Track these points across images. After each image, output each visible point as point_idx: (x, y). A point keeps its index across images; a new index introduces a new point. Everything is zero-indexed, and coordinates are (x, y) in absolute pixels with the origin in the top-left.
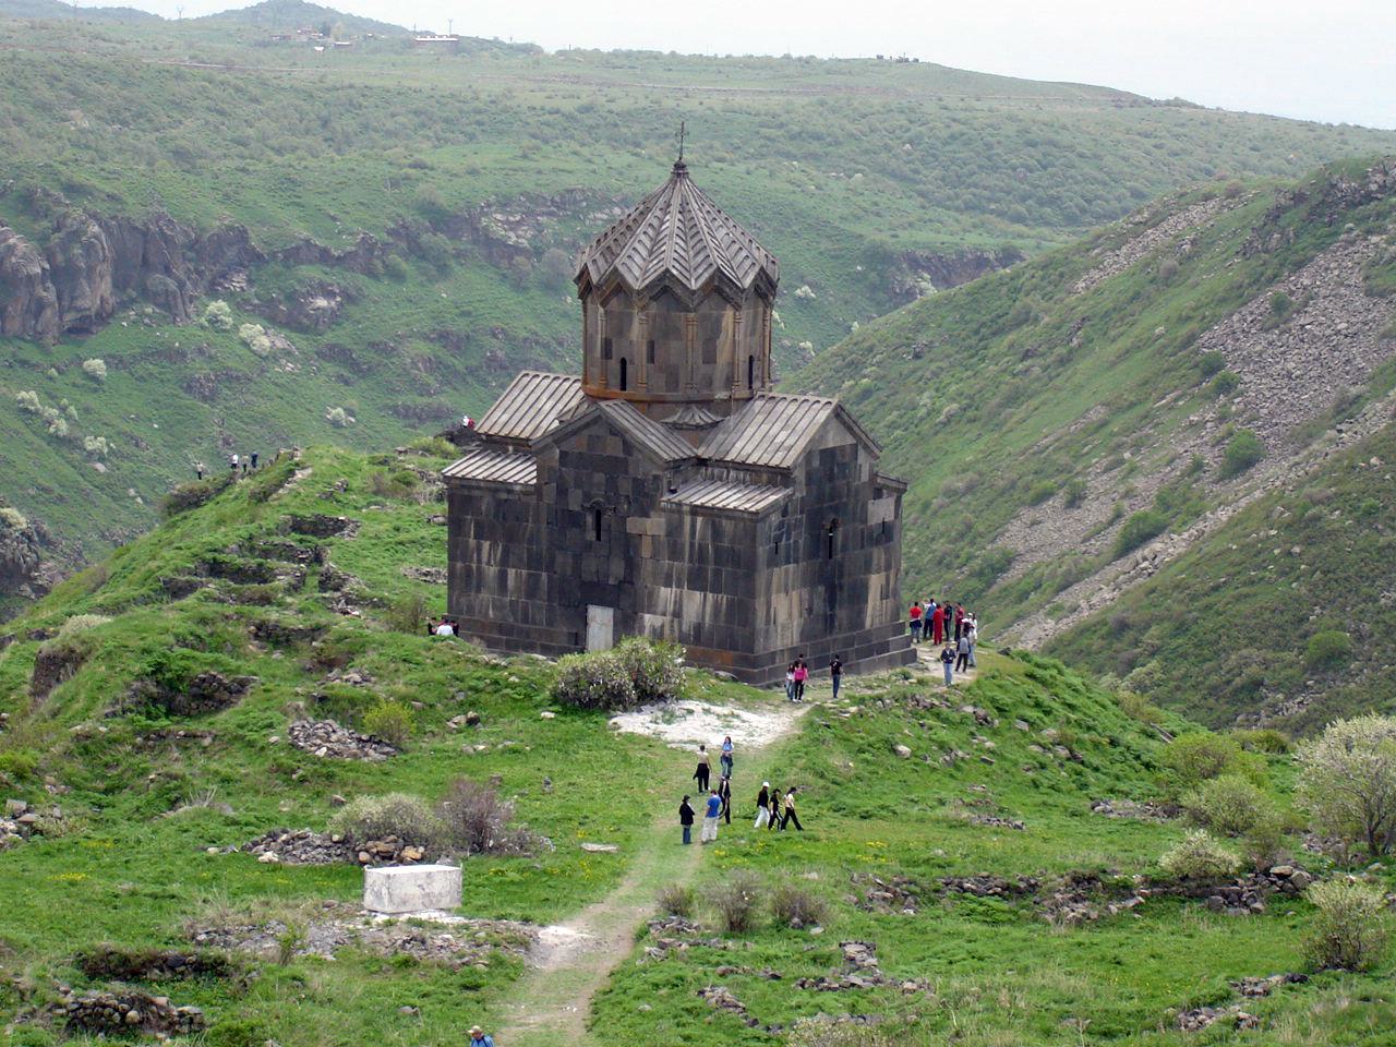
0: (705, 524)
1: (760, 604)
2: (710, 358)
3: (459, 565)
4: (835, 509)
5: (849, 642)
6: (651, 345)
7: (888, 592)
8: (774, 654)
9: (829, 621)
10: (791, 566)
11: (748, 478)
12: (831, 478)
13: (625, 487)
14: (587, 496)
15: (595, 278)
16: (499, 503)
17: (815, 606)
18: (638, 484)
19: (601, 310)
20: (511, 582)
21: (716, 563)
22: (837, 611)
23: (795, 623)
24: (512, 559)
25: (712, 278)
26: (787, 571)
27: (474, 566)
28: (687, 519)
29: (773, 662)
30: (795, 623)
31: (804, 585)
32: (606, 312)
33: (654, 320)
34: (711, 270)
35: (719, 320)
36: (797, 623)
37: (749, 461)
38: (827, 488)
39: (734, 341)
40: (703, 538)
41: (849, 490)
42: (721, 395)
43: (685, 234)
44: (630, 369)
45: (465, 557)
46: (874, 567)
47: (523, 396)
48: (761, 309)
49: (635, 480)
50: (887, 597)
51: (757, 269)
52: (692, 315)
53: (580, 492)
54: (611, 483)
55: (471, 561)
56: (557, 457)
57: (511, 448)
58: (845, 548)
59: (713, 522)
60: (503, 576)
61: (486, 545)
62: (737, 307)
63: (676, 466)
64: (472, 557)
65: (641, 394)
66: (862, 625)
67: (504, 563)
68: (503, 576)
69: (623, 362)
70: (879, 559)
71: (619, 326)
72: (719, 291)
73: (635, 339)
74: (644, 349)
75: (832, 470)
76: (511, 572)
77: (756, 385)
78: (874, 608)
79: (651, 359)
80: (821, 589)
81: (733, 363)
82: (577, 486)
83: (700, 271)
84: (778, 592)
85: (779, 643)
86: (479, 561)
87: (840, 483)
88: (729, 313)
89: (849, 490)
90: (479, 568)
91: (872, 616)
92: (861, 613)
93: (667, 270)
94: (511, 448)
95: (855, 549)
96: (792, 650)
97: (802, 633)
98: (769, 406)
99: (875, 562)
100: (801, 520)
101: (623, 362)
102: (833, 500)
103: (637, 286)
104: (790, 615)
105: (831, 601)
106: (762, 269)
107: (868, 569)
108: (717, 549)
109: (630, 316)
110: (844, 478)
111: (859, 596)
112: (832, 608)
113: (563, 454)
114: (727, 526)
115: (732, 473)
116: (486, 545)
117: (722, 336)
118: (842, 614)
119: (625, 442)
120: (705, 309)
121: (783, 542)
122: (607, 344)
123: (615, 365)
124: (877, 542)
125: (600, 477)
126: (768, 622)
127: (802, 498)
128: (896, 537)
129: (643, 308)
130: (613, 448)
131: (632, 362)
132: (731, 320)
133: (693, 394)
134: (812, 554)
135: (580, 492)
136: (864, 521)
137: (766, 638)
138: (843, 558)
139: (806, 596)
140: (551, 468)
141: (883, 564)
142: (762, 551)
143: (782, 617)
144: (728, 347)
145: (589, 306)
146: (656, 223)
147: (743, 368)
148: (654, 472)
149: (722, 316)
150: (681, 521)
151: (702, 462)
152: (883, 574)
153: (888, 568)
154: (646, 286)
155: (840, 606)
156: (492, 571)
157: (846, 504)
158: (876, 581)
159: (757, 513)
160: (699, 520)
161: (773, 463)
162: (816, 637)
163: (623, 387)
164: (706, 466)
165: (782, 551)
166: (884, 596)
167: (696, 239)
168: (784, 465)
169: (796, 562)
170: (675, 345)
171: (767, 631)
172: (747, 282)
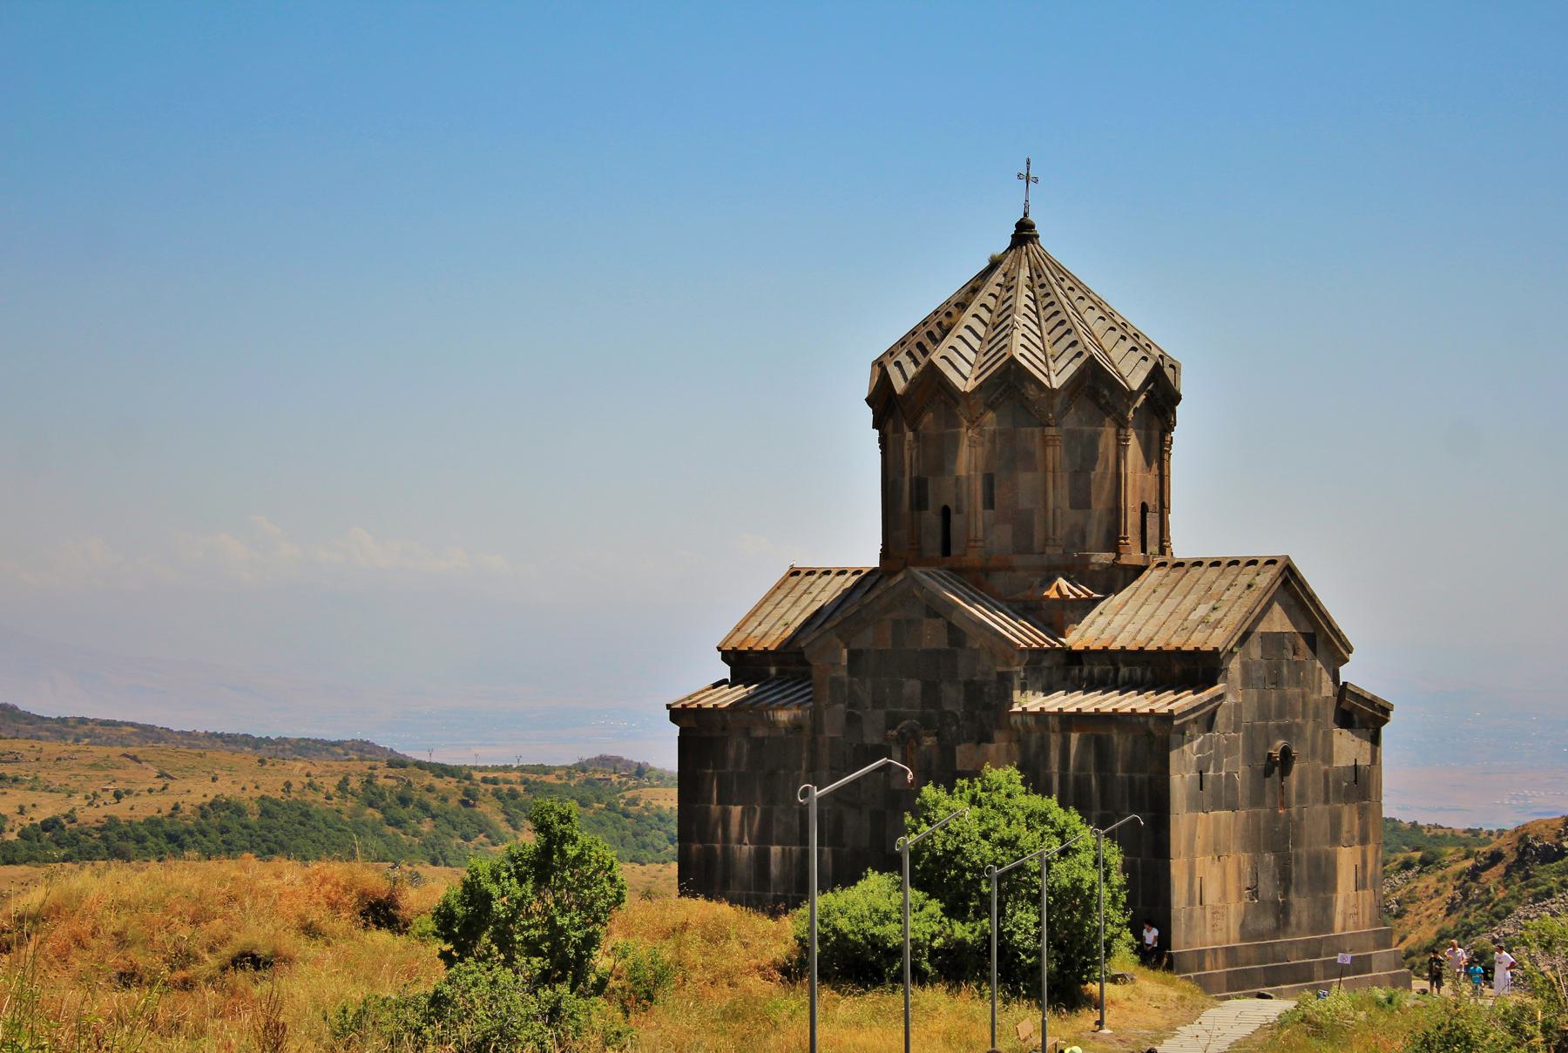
0: (1083, 743)
1: (1178, 868)
2: (1081, 501)
3: (695, 847)
4: (1285, 732)
5: (1312, 949)
6: (989, 481)
7: (1364, 878)
8: (1201, 953)
9: (1282, 912)
10: (1224, 814)
11: (1149, 674)
12: (1277, 682)
13: (953, 699)
14: (893, 721)
15: (899, 385)
16: (757, 744)
17: (1261, 885)
18: (973, 691)
19: (909, 435)
20: (774, 870)
21: (1103, 807)
22: (1293, 897)
23: (1232, 908)
24: (776, 830)
25: (1081, 372)
26: (1216, 819)
27: (718, 846)
28: (1055, 740)
29: (1201, 967)
30: (1232, 908)
31: (1245, 851)
32: (917, 438)
33: (993, 442)
34: (1079, 362)
35: (1093, 441)
36: (1234, 910)
37: (1152, 647)
38: (1274, 696)
39: (1118, 475)
40: (1081, 767)
41: (1305, 705)
42: (1103, 558)
43: (1037, 314)
44: (955, 518)
45: (705, 835)
46: (1344, 835)
47: (791, 599)
48: (1156, 434)
49: (969, 684)
50: (1364, 887)
51: (1150, 364)
52: (1051, 431)
53: (881, 713)
54: (931, 691)
55: (713, 839)
56: (845, 662)
57: (773, 670)
58: (1301, 797)
59: (1098, 740)
60: (762, 858)
61: (736, 811)
62: (1121, 424)
63: (1035, 656)
64: (715, 832)
65: (973, 558)
66: (1331, 929)
67: (763, 839)
68: (762, 858)
69: (946, 512)
70: (1352, 825)
71: (940, 455)
72: (1094, 395)
73: (964, 473)
74: (978, 487)
75: (1279, 668)
76: (775, 850)
77: (1153, 548)
78: (1346, 901)
79: (989, 502)
80: (1269, 858)
81: (1118, 508)
82: (878, 704)
83: (1061, 363)
84: (1205, 853)
85: (1208, 933)
86: (726, 838)
87: (1292, 691)
88: (1109, 432)
89: (1305, 705)
90: (725, 849)
91: (1344, 913)
92: (1327, 907)
93: (1012, 359)
94: (773, 670)
95: (1316, 801)
96: (1230, 952)
97: (1243, 926)
98: (1175, 574)
99: (1345, 827)
100: (1237, 739)
101: (946, 512)
102: (1281, 715)
103: (966, 386)
104: (1224, 894)
105: (1285, 880)
106: (1157, 364)
107: (1335, 839)
108: (1103, 783)
109: (956, 440)
110: (1298, 683)
111: (1323, 879)
112: (1286, 892)
113: (854, 656)
114: (1120, 741)
115: (1124, 671)
116: (736, 811)
117: (1099, 468)
118: (1300, 905)
119: (951, 628)
120: (1070, 421)
121: (1211, 773)
122: (920, 485)
123: (932, 518)
124: (1347, 797)
125: (912, 687)
126: (1191, 902)
127: (1238, 706)
128: (1373, 794)
129: (973, 422)
130: (932, 636)
131: (958, 511)
132: (1112, 442)
133: (1054, 553)
134: (1256, 800)
135: (881, 713)
136: (1328, 758)
137: (1190, 928)
138: (1300, 812)
139: (1247, 869)
140: (834, 680)
141: (1356, 832)
142: (1181, 780)
143: (1211, 895)
144: (1108, 485)
145: (891, 436)
146: (991, 302)
147: (1132, 518)
148: (1000, 669)
149: (1099, 434)
150: (1044, 748)
151: (1075, 657)
152: (1358, 848)
153: (1364, 840)
154: (980, 386)
155: (1297, 890)
156: (746, 850)
157: (1300, 728)
158: (1347, 859)
159: (1169, 716)
160: (1075, 737)
161: (1189, 647)
162: (1261, 936)
163: (946, 549)
164: (1081, 663)
165: (1208, 785)
166: (1360, 885)
167: (1051, 310)
168: (1208, 647)
169: (1233, 807)
170: (1025, 479)
171: (1190, 917)
172: (1135, 383)
